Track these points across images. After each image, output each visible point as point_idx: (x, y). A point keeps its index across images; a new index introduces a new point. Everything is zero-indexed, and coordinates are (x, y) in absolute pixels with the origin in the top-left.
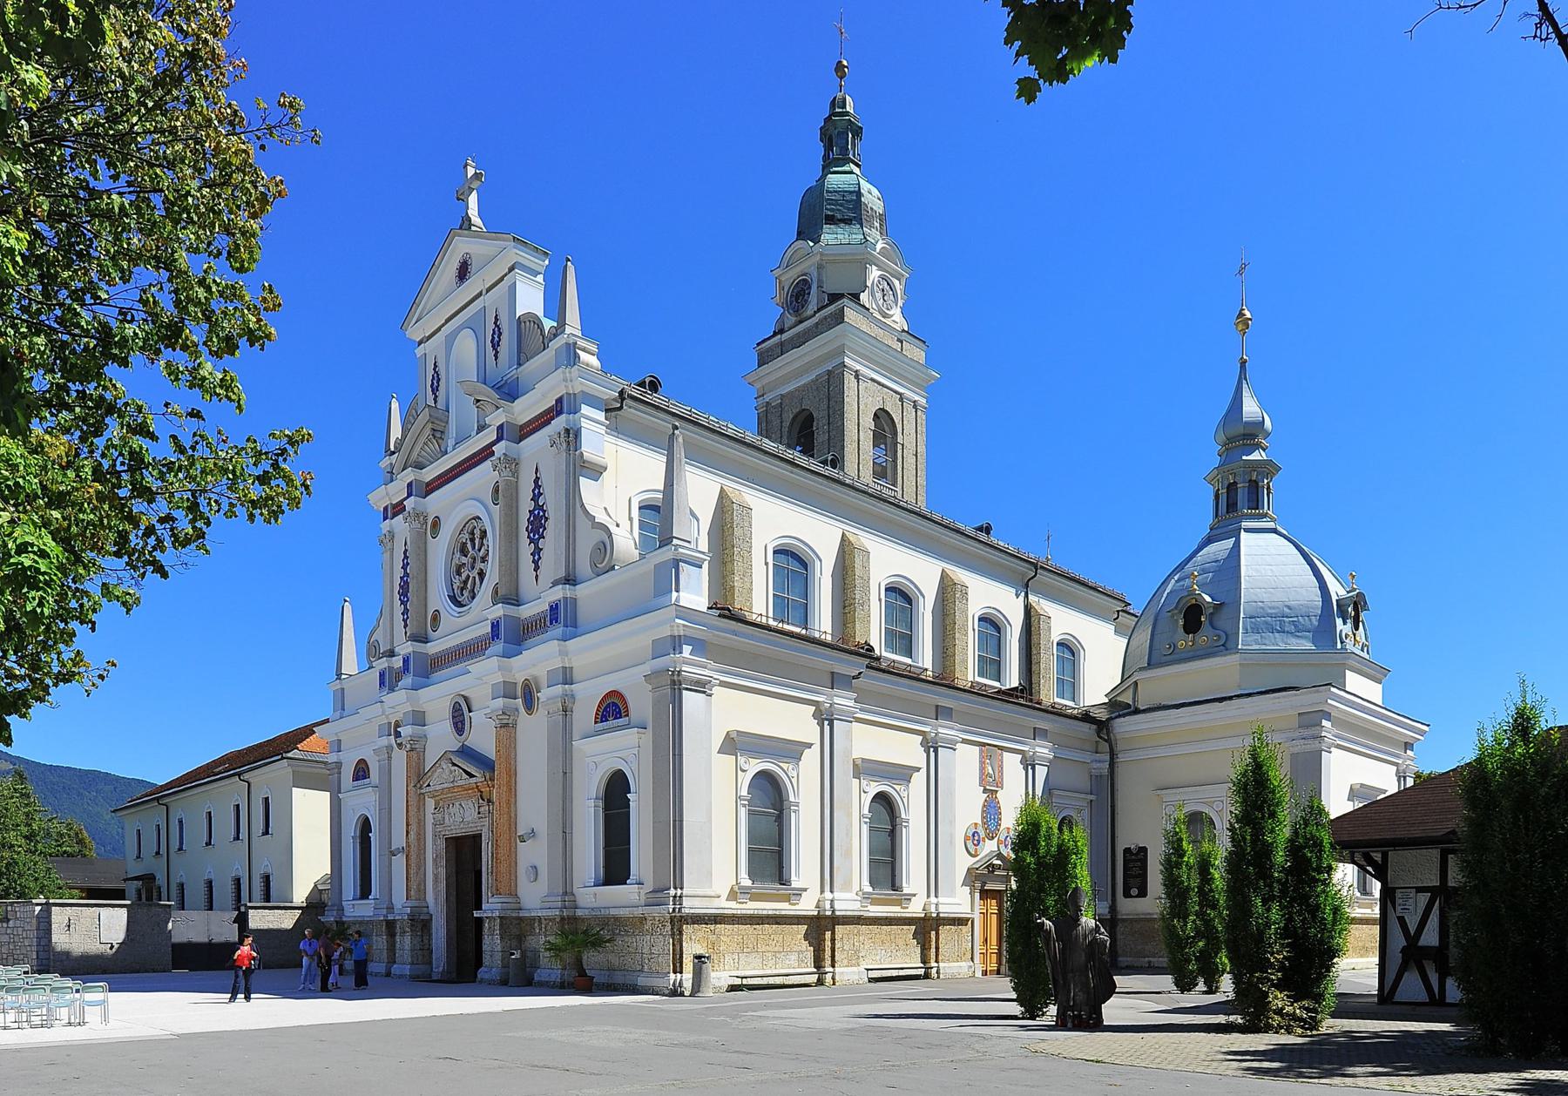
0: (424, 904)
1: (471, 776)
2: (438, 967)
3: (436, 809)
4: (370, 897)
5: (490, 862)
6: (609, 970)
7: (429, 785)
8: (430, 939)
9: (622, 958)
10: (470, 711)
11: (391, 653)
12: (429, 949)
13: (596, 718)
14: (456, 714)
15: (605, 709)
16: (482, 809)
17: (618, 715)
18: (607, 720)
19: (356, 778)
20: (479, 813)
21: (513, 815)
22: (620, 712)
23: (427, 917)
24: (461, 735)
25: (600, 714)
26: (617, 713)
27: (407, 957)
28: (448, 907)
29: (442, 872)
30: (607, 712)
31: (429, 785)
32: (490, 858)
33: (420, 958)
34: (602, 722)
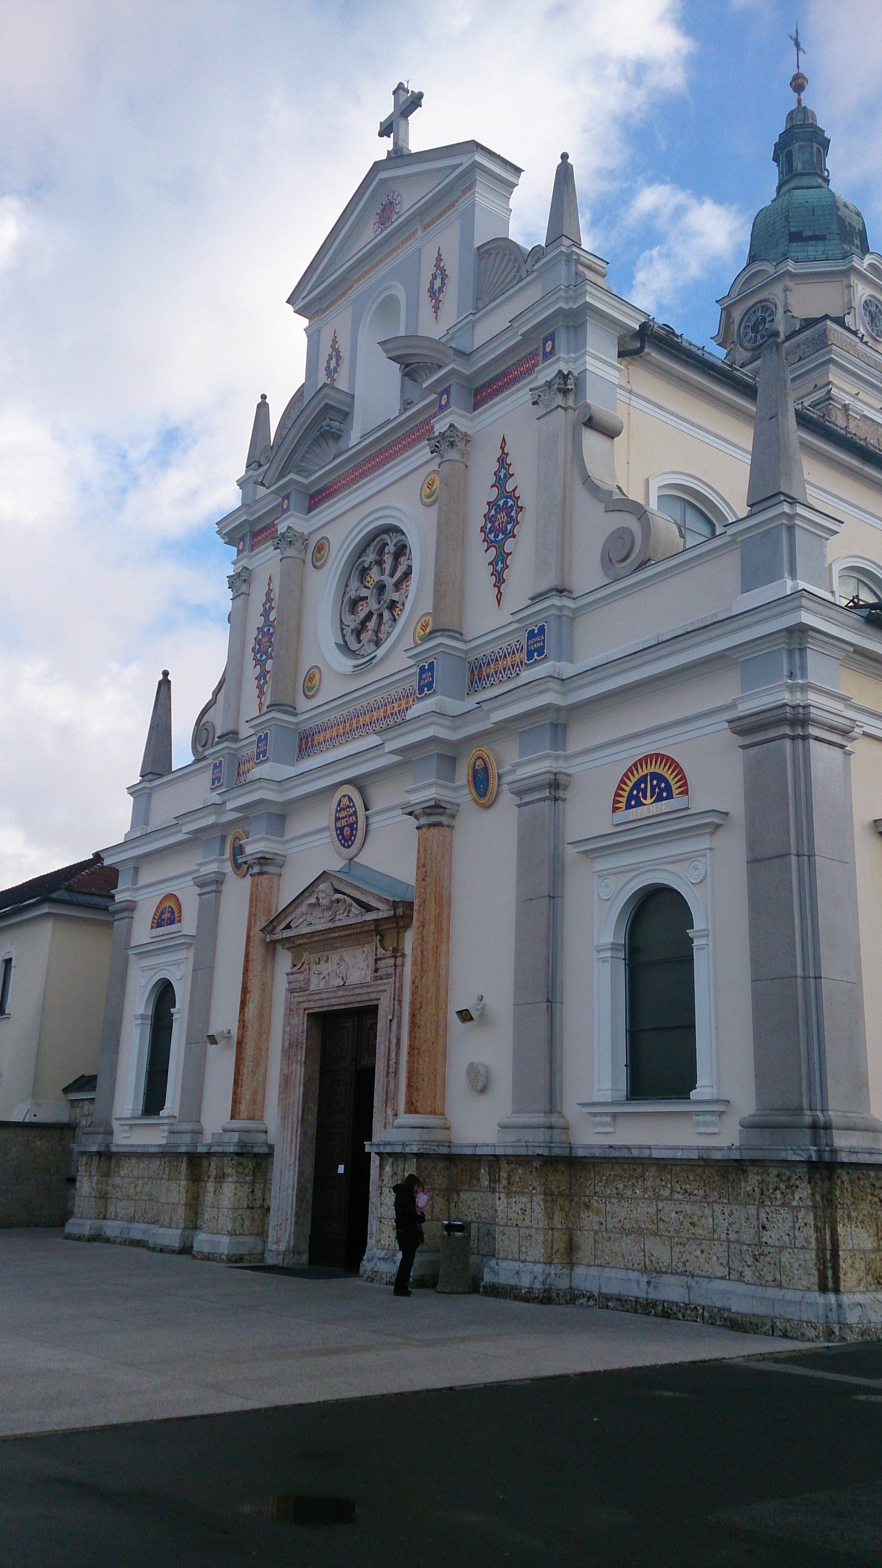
0: (262, 1127)
1: (368, 908)
2: (278, 1242)
3: (295, 966)
4: (162, 1113)
5: (393, 1055)
6: (645, 1270)
7: (288, 927)
8: (266, 1189)
9: (677, 1249)
10: (367, 809)
11: (232, 735)
12: (262, 1206)
13: (615, 802)
14: (342, 814)
15: (636, 786)
16: (382, 964)
17: (663, 792)
18: (639, 804)
19: (158, 922)
20: (376, 970)
21: (442, 973)
22: (668, 788)
23: (265, 1150)
24: (349, 847)
25: (625, 794)
26: (662, 791)
27: (226, 1222)
28: (304, 1134)
29: (299, 1072)
30: (639, 790)
31: (288, 927)
32: (393, 1048)
33: (247, 1222)
34: (629, 807)
